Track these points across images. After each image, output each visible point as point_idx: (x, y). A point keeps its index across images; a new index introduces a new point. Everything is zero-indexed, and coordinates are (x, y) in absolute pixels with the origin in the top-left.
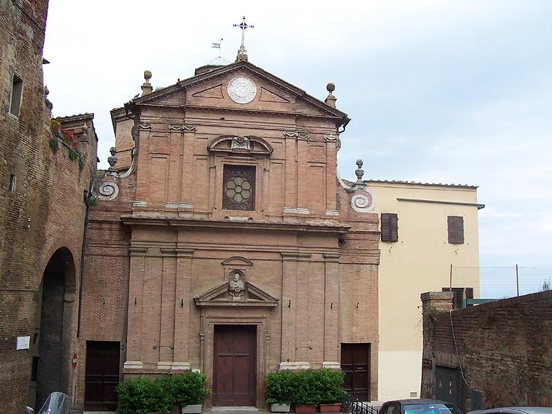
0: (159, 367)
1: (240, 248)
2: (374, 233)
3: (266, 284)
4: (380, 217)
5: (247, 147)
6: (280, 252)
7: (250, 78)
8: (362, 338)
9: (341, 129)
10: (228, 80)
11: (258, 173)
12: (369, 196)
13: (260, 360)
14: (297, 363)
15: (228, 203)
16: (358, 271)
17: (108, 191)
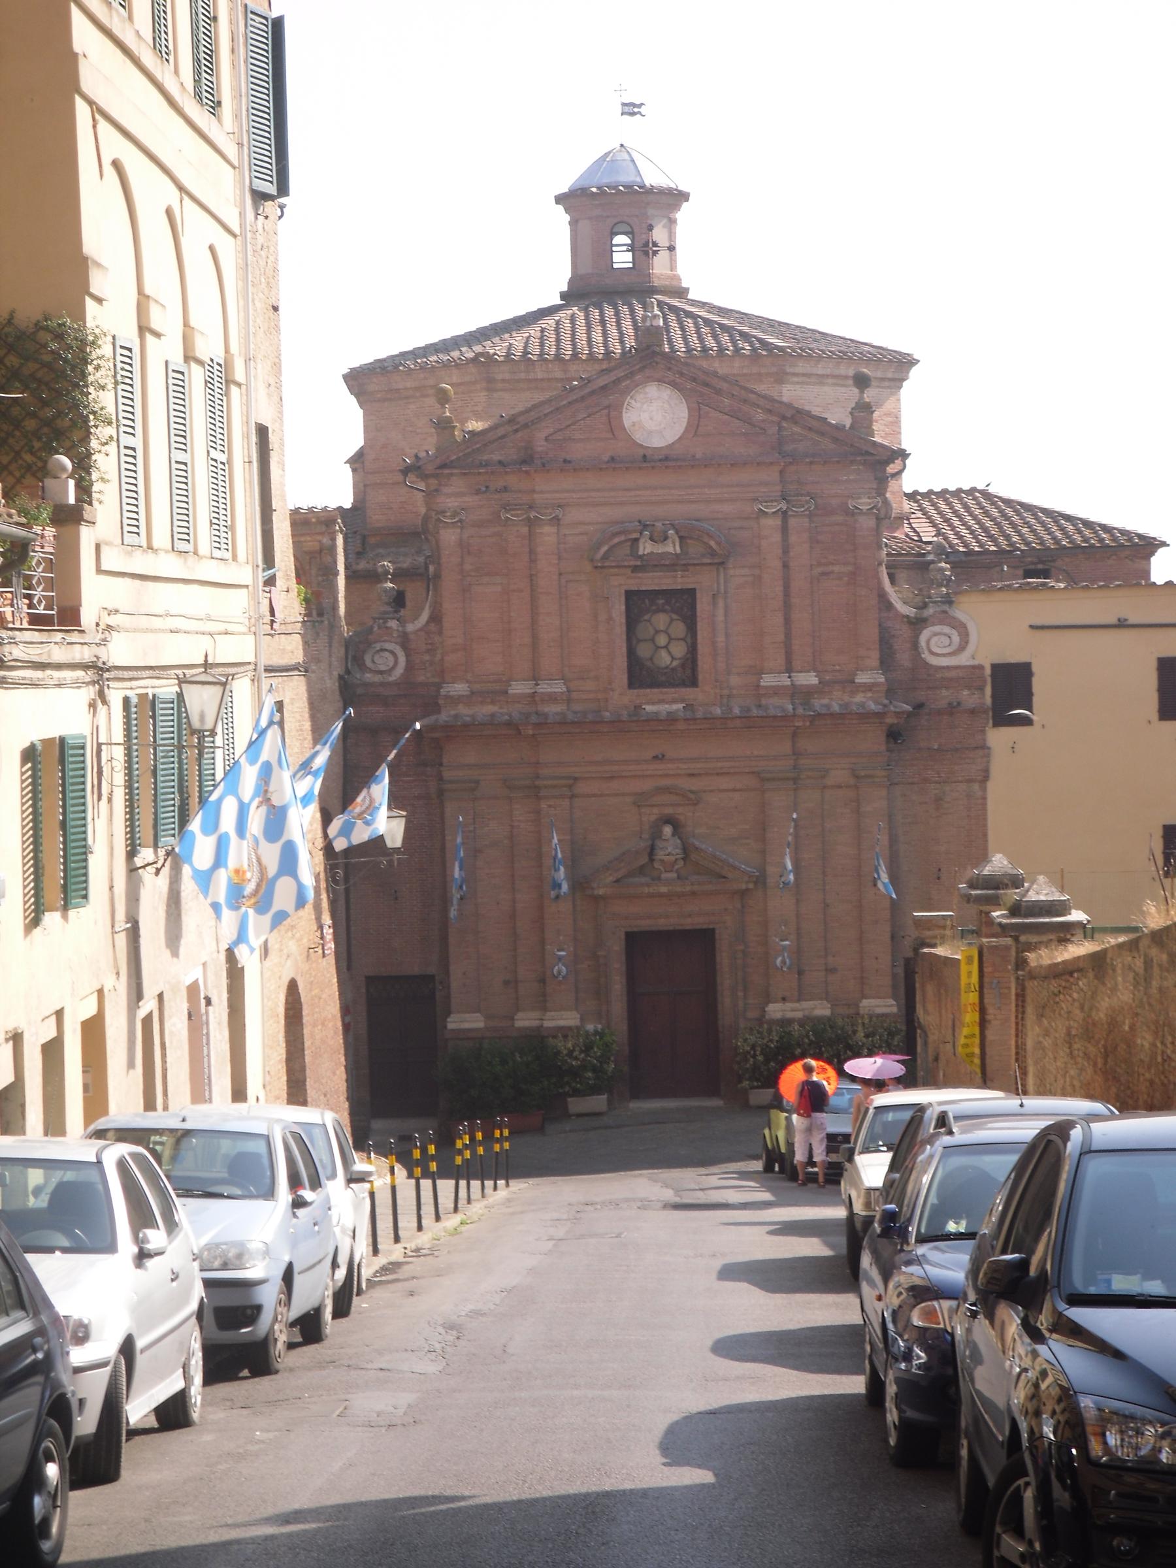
0: (519, 1024)
4: (988, 671)
5: (672, 547)
6: (756, 774)
7: (674, 385)
9: (891, 469)
11: (703, 605)
13: (725, 1001)
14: (806, 1004)
15: (640, 674)
16: (938, 800)
17: (383, 662)
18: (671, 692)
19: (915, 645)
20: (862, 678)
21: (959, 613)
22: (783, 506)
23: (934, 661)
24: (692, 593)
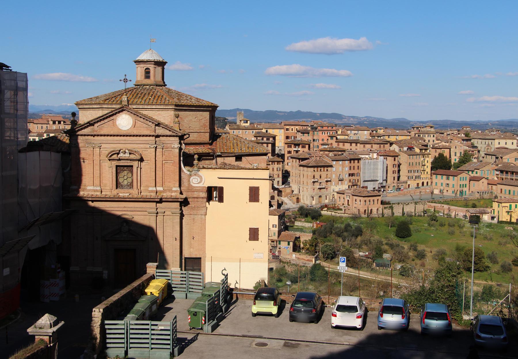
1: (126, 209)
2: (202, 198)
5: (127, 155)
8: (196, 255)
12: (200, 177)
18: (126, 190)
19: (189, 181)
20: (174, 189)
22: (155, 146)
24: (132, 166)
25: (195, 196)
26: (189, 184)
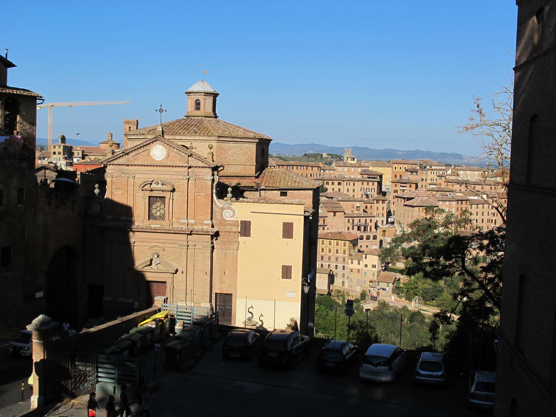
1: (157, 241)
2: (235, 232)
3: (172, 260)
5: (160, 186)
8: (227, 291)
10: (151, 147)
16: (226, 254)
19: (222, 214)
20: (205, 222)
21: (232, 207)
23: (226, 219)
25: (228, 230)
26: (222, 217)
